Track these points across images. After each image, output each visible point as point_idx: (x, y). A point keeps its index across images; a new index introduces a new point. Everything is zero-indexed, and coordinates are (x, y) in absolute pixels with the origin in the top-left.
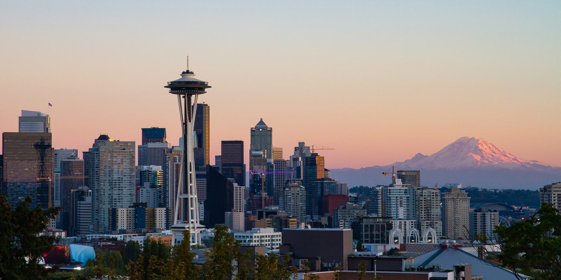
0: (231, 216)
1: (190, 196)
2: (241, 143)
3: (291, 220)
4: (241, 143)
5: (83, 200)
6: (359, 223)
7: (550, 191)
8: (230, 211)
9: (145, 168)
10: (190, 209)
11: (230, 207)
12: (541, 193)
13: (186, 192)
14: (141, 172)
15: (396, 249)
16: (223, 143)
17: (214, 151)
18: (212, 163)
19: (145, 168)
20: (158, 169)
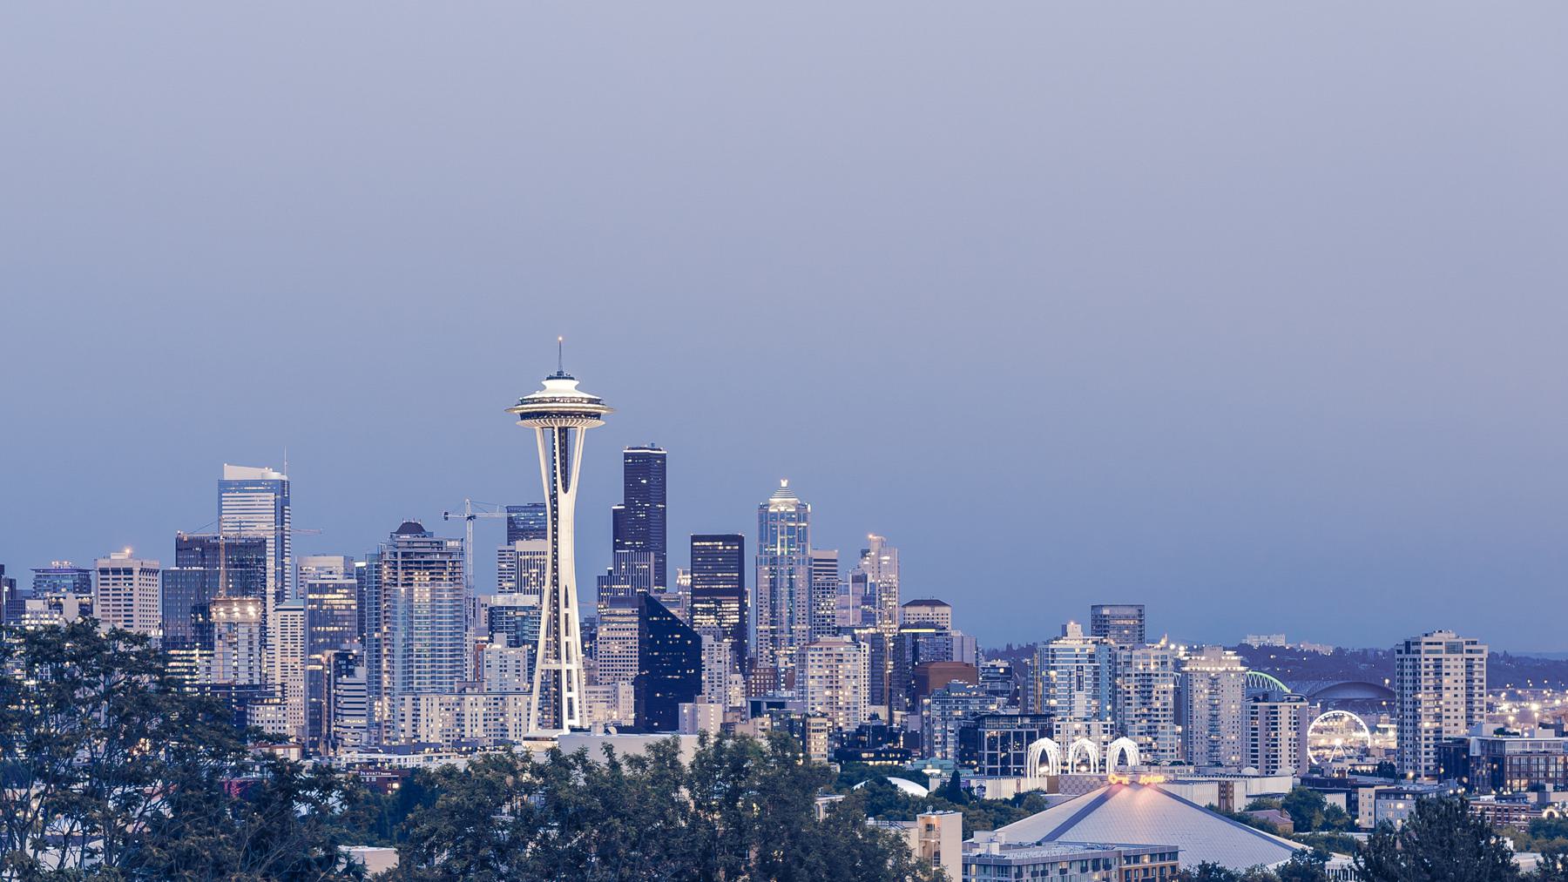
0: (694, 713)
1: (564, 667)
3: (813, 721)
5: (351, 673)
6: (976, 728)
7: (1419, 652)
8: (691, 700)
9: (500, 600)
10: (566, 695)
11: (691, 689)
12: (1398, 656)
13: (558, 657)
14: (491, 609)
15: (1038, 790)
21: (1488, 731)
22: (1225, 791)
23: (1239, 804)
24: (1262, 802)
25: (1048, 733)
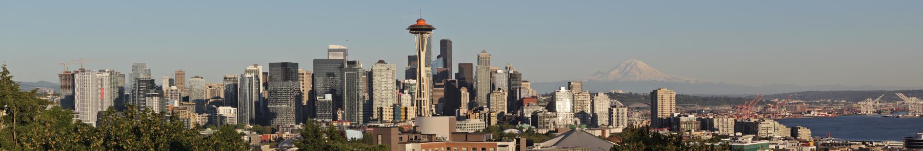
2: (471, 65)
4: (471, 65)
9: (406, 81)
16: (460, 65)
17: (455, 70)
18: (453, 78)
19: (406, 81)
20: (412, 81)
21: (676, 115)
22: (603, 132)
23: (607, 135)
24: (613, 136)
25: (556, 117)
